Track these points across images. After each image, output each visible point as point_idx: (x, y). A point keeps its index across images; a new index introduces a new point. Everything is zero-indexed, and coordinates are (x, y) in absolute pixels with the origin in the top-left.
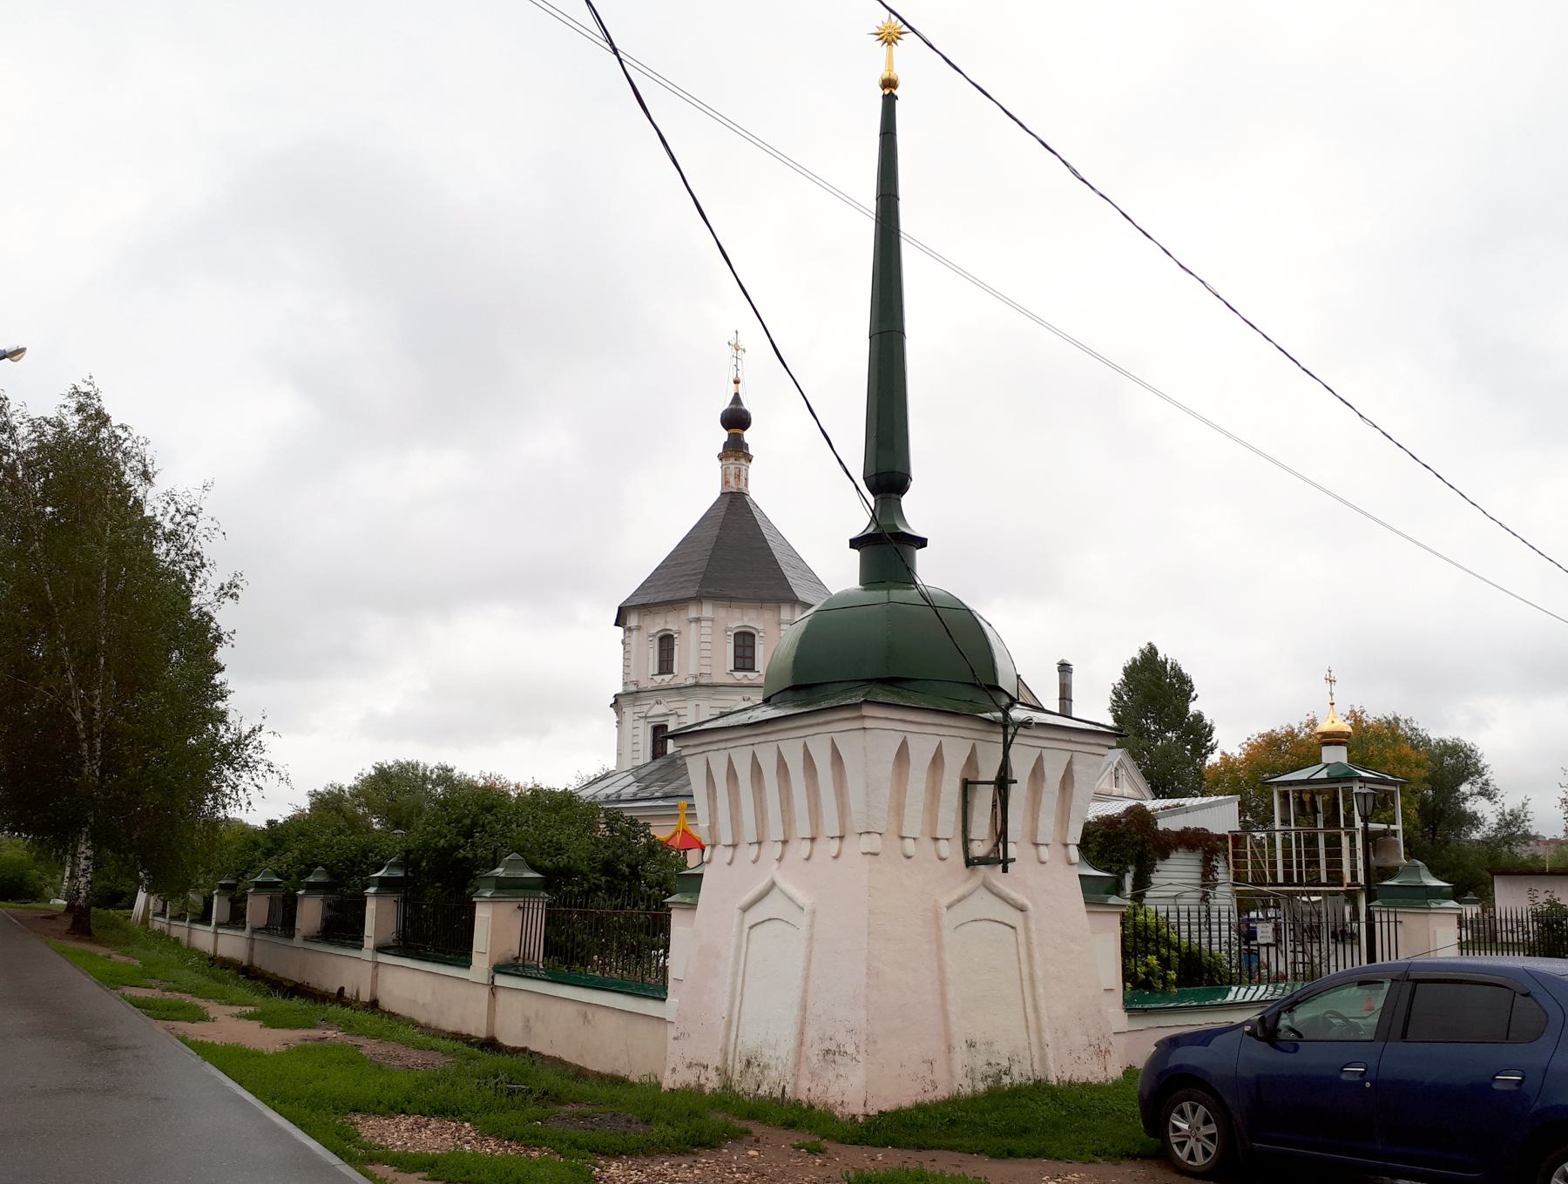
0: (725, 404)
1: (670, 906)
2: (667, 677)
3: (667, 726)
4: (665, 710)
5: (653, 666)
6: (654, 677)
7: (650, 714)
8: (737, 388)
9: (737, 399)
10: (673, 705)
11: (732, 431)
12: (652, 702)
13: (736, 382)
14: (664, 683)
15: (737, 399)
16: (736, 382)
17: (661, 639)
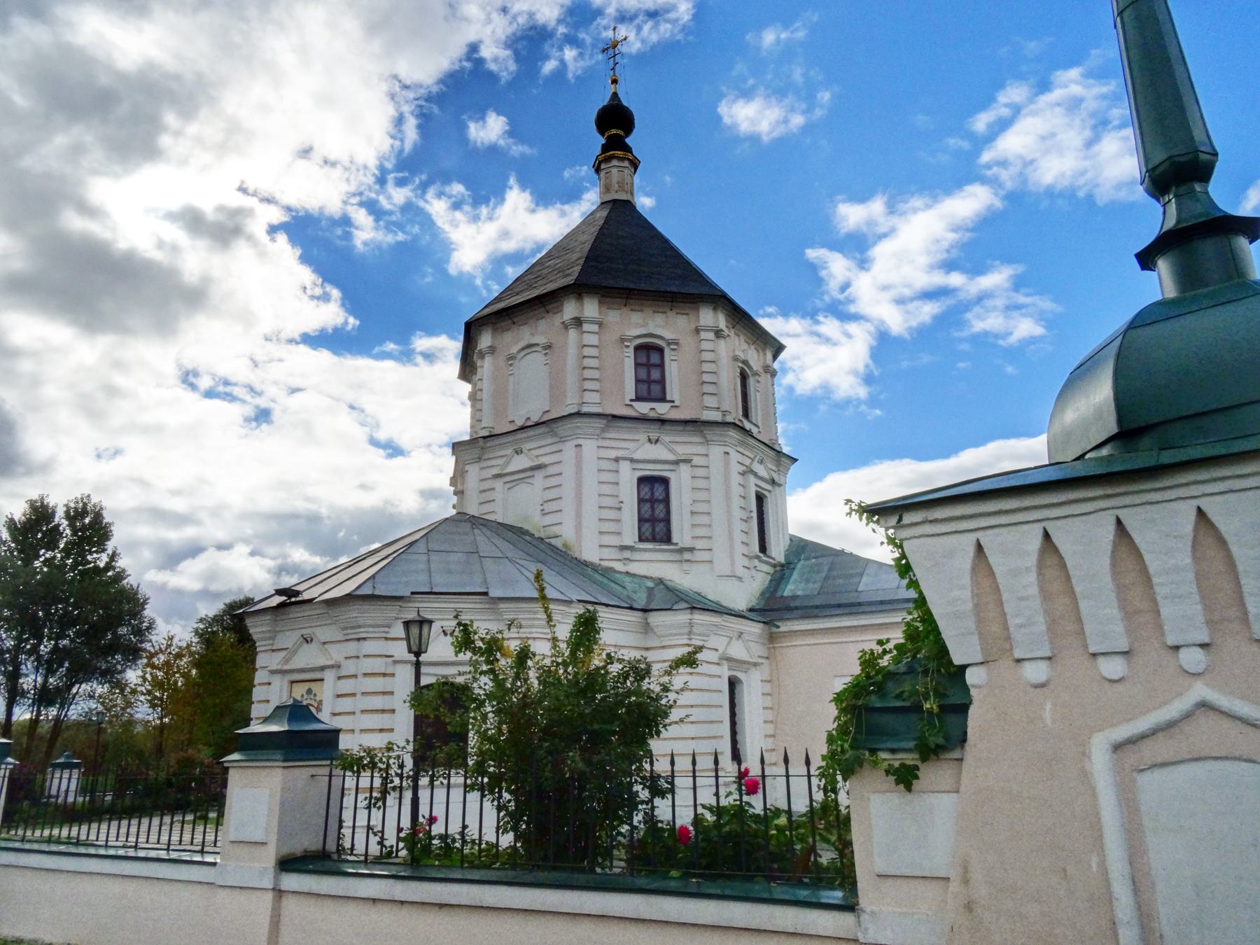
0: (604, 100)
1: (226, 765)
2: (662, 409)
3: (665, 482)
4: (671, 457)
5: (630, 390)
6: (633, 403)
7: (637, 456)
8: (616, 88)
9: (615, 95)
10: (683, 451)
11: (614, 131)
12: (642, 437)
13: (615, 82)
14: (652, 415)
15: (615, 95)
16: (615, 82)
17: (638, 349)
